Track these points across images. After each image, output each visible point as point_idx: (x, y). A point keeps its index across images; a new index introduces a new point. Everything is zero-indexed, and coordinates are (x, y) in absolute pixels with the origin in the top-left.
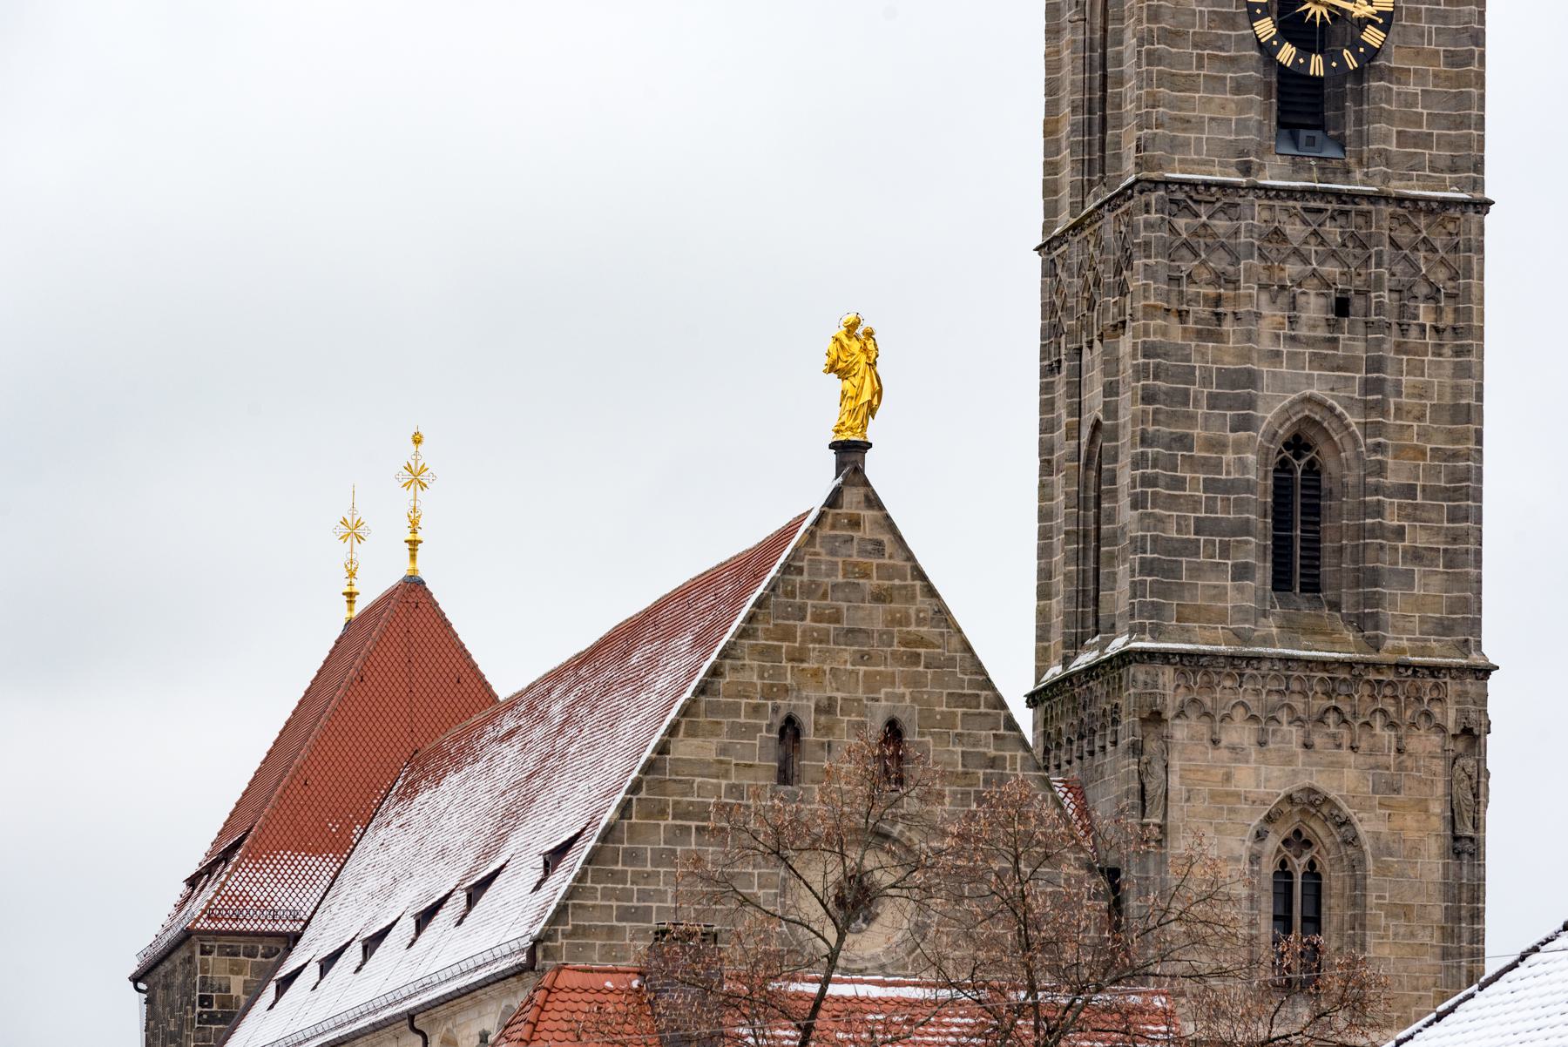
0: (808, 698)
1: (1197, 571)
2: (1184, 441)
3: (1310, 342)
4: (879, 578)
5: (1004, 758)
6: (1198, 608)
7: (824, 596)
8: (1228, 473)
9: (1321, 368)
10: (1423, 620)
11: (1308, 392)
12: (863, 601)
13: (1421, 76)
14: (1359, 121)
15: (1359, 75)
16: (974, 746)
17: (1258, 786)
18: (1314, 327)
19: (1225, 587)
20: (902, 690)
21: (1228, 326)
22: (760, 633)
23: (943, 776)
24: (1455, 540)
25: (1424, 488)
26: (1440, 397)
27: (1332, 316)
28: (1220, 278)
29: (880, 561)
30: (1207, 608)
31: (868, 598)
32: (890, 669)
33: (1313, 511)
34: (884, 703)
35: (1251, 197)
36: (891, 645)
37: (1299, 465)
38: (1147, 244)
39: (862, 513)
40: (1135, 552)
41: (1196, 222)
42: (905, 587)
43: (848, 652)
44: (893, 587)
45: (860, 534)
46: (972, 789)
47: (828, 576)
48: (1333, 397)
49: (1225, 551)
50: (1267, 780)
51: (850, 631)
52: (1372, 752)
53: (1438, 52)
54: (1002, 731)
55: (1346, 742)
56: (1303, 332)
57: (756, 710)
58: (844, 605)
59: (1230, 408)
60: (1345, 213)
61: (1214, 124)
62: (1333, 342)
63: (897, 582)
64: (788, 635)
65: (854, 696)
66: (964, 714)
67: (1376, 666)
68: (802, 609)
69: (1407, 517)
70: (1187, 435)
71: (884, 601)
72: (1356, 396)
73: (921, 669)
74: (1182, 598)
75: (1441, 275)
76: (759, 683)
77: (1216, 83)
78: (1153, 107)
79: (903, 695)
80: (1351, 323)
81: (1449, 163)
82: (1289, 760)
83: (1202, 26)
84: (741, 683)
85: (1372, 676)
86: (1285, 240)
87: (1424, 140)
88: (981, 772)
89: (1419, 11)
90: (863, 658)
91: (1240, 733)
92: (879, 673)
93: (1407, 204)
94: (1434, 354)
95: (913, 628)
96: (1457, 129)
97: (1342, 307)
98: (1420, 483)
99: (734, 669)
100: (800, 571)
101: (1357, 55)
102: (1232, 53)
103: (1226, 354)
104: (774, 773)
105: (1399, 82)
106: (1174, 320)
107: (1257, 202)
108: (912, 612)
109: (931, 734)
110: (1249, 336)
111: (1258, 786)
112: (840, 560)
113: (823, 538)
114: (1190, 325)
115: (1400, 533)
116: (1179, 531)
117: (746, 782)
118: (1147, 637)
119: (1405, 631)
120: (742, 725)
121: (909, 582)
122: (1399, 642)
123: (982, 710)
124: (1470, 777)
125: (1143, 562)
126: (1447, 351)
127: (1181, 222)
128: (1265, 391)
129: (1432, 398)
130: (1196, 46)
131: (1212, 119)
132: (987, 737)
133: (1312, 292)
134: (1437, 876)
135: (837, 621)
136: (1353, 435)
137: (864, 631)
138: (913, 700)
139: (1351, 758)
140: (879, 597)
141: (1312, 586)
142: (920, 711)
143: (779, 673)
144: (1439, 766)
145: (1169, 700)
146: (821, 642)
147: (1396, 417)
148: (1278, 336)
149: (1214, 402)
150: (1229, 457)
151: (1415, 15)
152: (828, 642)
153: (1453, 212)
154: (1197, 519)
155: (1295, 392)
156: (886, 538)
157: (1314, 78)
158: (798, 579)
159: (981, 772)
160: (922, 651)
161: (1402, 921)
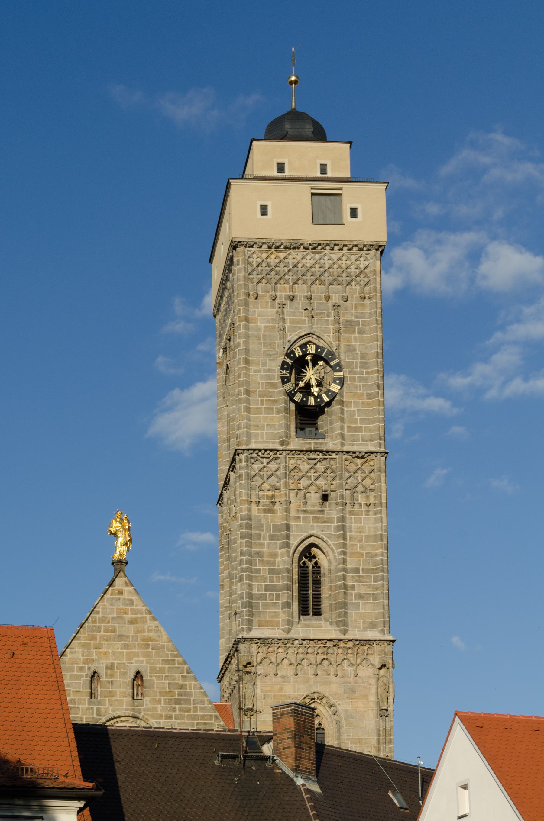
0: (102, 663)
1: (266, 606)
3: (312, 512)
4: (131, 614)
5: (186, 685)
6: (267, 621)
7: (109, 622)
8: (279, 566)
9: (317, 522)
10: (364, 623)
11: (312, 532)
12: (125, 624)
14: (331, 423)
16: (173, 680)
17: (294, 692)
18: (314, 506)
19: (278, 612)
20: (142, 659)
21: (277, 507)
22: (82, 638)
23: (160, 692)
24: (377, 589)
25: (363, 569)
26: (369, 532)
27: (321, 501)
29: (132, 607)
31: (127, 622)
32: (137, 650)
34: (134, 664)
35: (284, 454)
36: (137, 641)
37: (310, 565)
39: (124, 588)
40: (240, 599)
41: (262, 465)
42: (142, 617)
43: (119, 644)
44: (137, 618)
45: (123, 597)
46: (173, 698)
47: (110, 614)
48: (323, 534)
49: (278, 597)
50: (298, 689)
51: (120, 636)
52: (343, 676)
53: (363, 394)
54: (185, 674)
55: (332, 672)
56: (309, 508)
57: (81, 669)
58: (117, 625)
59: (278, 540)
60: (325, 459)
61: (269, 427)
63: (139, 616)
64: (93, 638)
65: (122, 662)
66: (169, 668)
68: (99, 628)
69: (356, 581)
70: (261, 552)
71: (134, 623)
72: (333, 533)
73: (150, 650)
74: (260, 617)
76: (82, 658)
77: (269, 410)
78: (242, 421)
79: (142, 661)
80: (330, 504)
81: (370, 438)
82: (307, 681)
83: (262, 388)
84: (73, 658)
87: (357, 429)
88: (176, 691)
89: (355, 378)
90: (125, 646)
91: (286, 670)
92: (133, 652)
93: (351, 454)
94: (366, 515)
95: (146, 634)
96: (373, 424)
97: (325, 497)
98: (361, 567)
99: (71, 653)
100: (98, 613)
101: (328, 396)
102: (276, 398)
104: (89, 694)
105: (347, 406)
106: (254, 506)
107: (288, 456)
108: (146, 628)
109: (155, 676)
110: (287, 510)
111: (294, 692)
112: (115, 607)
113: (108, 599)
115: (353, 587)
116: (258, 590)
117: (77, 698)
118: (245, 633)
119: (356, 627)
120: (76, 675)
121: (144, 615)
122: (354, 633)
123: (176, 666)
124: (385, 685)
125: (242, 603)
126: (371, 513)
128: (293, 533)
129: (365, 533)
130: (260, 396)
131: (268, 425)
132: (179, 676)
133: (313, 492)
134: (373, 726)
135: (114, 632)
137: (126, 636)
138: (147, 663)
139: (334, 679)
142: (150, 667)
144: (373, 681)
145: (255, 658)
146: (107, 641)
147: (350, 541)
148: (298, 510)
149: (272, 538)
150: (279, 559)
151: (353, 379)
152: (110, 641)
153: (372, 456)
154: (266, 585)
155: (306, 532)
156: (135, 598)
157: (310, 406)
158: (97, 616)
159: (176, 691)
160: (150, 643)
161: (358, 745)
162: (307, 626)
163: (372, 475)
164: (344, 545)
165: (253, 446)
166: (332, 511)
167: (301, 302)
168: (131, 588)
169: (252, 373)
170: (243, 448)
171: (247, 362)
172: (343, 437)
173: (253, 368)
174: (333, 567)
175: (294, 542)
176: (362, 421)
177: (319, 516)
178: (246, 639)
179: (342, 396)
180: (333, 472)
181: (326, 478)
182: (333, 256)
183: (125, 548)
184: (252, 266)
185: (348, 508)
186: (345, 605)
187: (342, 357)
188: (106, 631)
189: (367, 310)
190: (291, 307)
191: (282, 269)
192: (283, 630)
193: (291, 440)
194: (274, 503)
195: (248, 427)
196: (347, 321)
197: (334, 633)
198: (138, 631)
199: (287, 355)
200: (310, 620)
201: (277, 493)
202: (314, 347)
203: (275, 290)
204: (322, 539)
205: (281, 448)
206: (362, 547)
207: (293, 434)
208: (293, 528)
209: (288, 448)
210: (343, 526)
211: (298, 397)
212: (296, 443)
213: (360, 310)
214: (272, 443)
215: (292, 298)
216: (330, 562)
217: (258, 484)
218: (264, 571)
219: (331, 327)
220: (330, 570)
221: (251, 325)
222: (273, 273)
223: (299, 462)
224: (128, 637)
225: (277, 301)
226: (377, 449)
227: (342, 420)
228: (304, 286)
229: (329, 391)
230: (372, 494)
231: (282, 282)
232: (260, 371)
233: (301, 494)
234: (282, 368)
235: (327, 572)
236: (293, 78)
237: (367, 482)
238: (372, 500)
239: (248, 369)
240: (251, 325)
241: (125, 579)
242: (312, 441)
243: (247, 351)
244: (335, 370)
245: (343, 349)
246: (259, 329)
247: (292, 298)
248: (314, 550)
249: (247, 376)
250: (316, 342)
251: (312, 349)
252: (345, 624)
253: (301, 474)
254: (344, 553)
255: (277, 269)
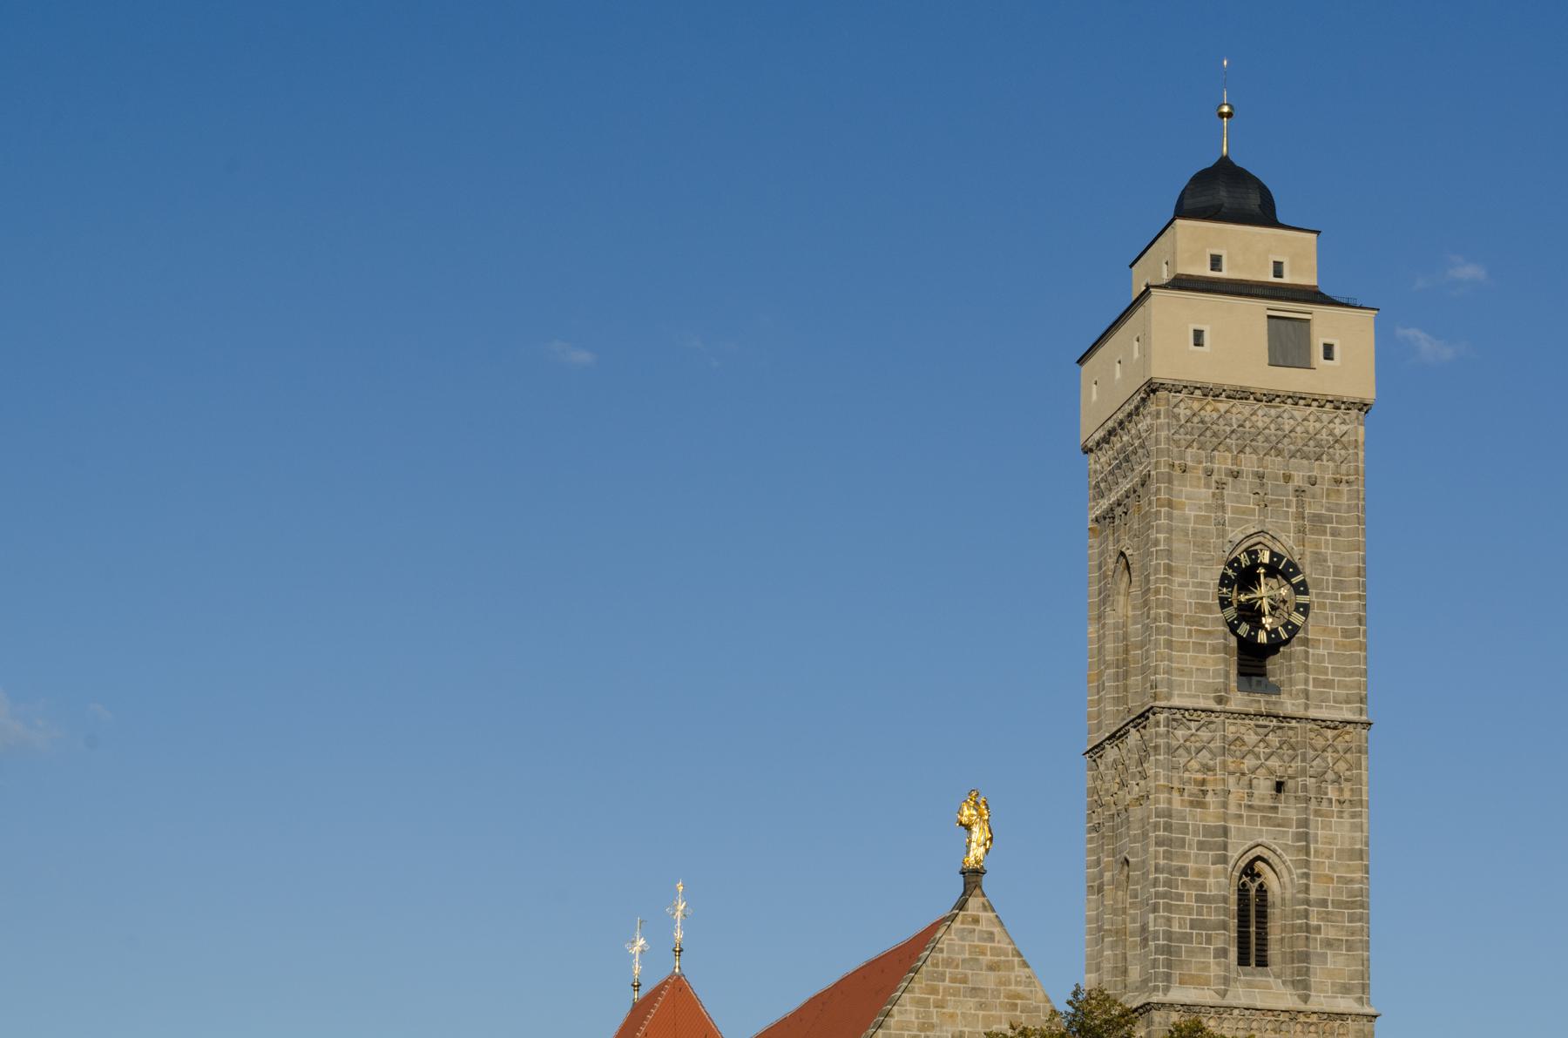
1: (1190, 952)
2: (1182, 871)
3: (1261, 809)
10: (1333, 985)
13: (1327, 644)
14: (1290, 671)
15: (1287, 642)
21: (1210, 798)
24: (1353, 934)
28: (1207, 768)
30: (1198, 976)
33: (1262, 915)
37: (1253, 887)
38: (1156, 748)
43: (972, 1002)
49: (1209, 941)
56: (1256, 802)
62: (1275, 809)
64: (934, 991)
67: (1306, 1014)
68: (943, 974)
69: (1323, 919)
75: (1341, 766)
77: (1200, 647)
85: (1302, 1018)
86: (1244, 743)
87: (1328, 684)
90: (981, 1006)
95: (1013, 987)
97: (1279, 787)
99: (900, 1012)
100: (941, 951)
103: (1211, 816)
106: (1175, 795)
110: (1225, 805)
114: (1186, 797)
115: (1318, 929)
125: (1157, 947)
127: (1180, 733)
128: (1232, 840)
136: (1288, 868)
140: (991, 968)
141: (1262, 962)
143: (928, 1015)
149: (1201, 846)
150: (1211, 880)
151: (1322, 606)
153: (1349, 728)
156: (996, 930)
162: (1249, 985)
163: (1348, 756)
164: (1307, 864)
165: (1176, 702)
166: (1290, 810)
167: (1248, 481)
168: (992, 915)
169: (1175, 587)
170: (1162, 704)
171: (1169, 570)
172: (1306, 694)
173: (1177, 579)
174: (1288, 896)
175: (1233, 854)
176: (1336, 671)
177: (1270, 815)
178: (1163, 1004)
179: (1306, 632)
180: (1293, 748)
181: (1281, 758)
182: (1296, 413)
183: (982, 849)
184: (1178, 420)
185: (1313, 805)
186: (1305, 957)
187: (1307, 571)
188: (953, 980)
189: (1344, 500)
190: (1234, 488)
191: (1221, 427)
192: (1217, 992)
193: (1231, 696)
194: (1204, 793)
195: (1169, 671)
196: (1315, 515)
197: (1287, 999)
198: (1001, 983)
199: (1230, 565)
200: (1252, 973)
201: (1209, 777)
202: (1267, 554)
203: (1212, 460)
204: (1274, 852)
205: (1218, 708)
206: (1331, 867)
207: (1234, 685)
208: (1233, 833)
209: (1227, 708)
210: (1307, 834)
211: (1244, 629)
212: (1238, 701)
213: (1333, 499)
214: (1205, 698)
215: (1236, 475)
216: (1282, 886)
217: (1182, 761)
218: (1189, 897)
219: (1292, 522)
220: (1283, 899)
221: (1176, 512)
222: (1208, 433)
223: (1243, 730)
224: (985, 991)
225: (1214, 477)
226: (1355, 718)
227: (1307, 669)
228: (1254, 457)
229: (1289, 622)
230: (1346, 786)
231: (1221, 448)
232: (1187, 585)
233: (1245, 779)
234: (1222, 584)
235: (1278, 901)
236: (1226, 109)
237: (1341, 766)
238: (1347, 795)
239: (1169, 581)
240: (1176, 512)
241: (982, 899)
242: (1262, 698)
243: (1169, 553)
244: (1298, 592)
245: (1308, 558)
246: (1186, 520)
247: (1236, 475)
248: (1260, 865)
249: (1168, 591)
250: (1270, 544)
251: (1265, 558)
252: (1307, 987)
253: (1245, 748)
254: (1307, 876)
255: (1215, 427)
